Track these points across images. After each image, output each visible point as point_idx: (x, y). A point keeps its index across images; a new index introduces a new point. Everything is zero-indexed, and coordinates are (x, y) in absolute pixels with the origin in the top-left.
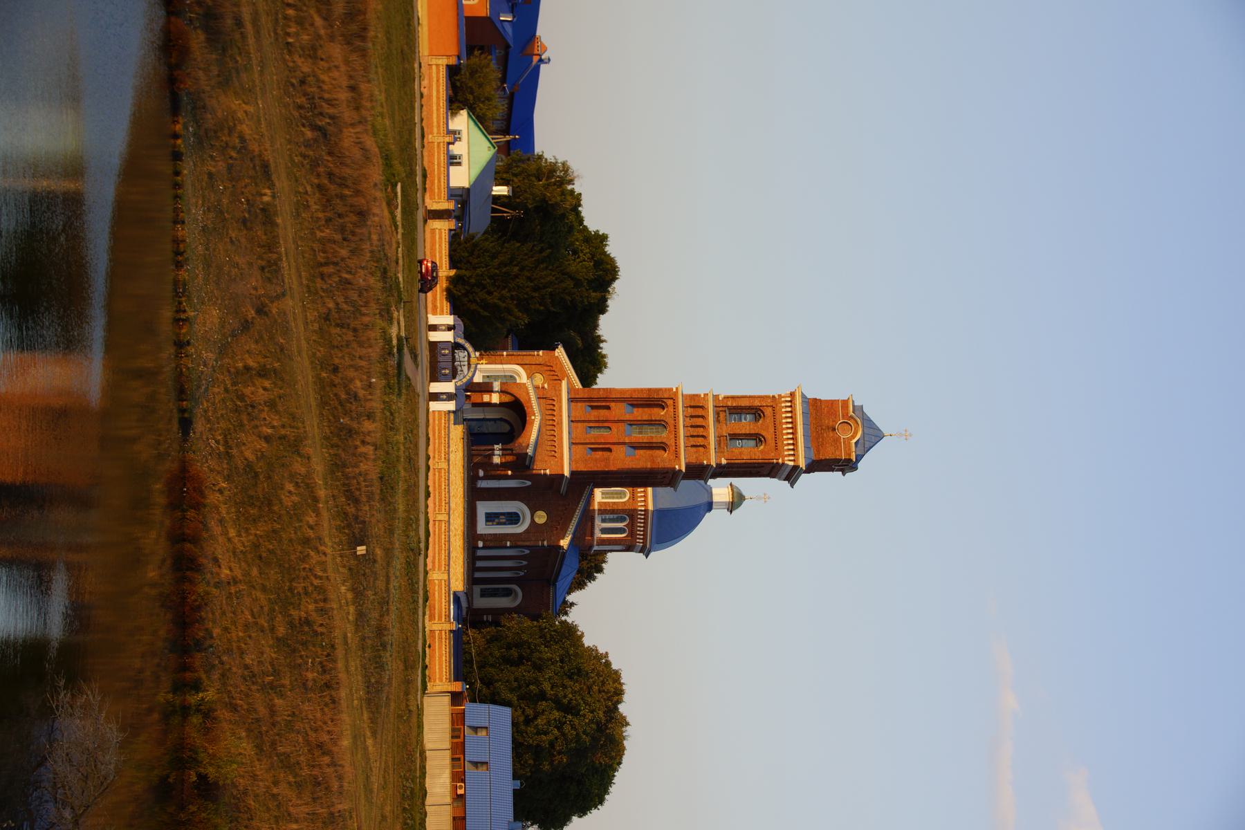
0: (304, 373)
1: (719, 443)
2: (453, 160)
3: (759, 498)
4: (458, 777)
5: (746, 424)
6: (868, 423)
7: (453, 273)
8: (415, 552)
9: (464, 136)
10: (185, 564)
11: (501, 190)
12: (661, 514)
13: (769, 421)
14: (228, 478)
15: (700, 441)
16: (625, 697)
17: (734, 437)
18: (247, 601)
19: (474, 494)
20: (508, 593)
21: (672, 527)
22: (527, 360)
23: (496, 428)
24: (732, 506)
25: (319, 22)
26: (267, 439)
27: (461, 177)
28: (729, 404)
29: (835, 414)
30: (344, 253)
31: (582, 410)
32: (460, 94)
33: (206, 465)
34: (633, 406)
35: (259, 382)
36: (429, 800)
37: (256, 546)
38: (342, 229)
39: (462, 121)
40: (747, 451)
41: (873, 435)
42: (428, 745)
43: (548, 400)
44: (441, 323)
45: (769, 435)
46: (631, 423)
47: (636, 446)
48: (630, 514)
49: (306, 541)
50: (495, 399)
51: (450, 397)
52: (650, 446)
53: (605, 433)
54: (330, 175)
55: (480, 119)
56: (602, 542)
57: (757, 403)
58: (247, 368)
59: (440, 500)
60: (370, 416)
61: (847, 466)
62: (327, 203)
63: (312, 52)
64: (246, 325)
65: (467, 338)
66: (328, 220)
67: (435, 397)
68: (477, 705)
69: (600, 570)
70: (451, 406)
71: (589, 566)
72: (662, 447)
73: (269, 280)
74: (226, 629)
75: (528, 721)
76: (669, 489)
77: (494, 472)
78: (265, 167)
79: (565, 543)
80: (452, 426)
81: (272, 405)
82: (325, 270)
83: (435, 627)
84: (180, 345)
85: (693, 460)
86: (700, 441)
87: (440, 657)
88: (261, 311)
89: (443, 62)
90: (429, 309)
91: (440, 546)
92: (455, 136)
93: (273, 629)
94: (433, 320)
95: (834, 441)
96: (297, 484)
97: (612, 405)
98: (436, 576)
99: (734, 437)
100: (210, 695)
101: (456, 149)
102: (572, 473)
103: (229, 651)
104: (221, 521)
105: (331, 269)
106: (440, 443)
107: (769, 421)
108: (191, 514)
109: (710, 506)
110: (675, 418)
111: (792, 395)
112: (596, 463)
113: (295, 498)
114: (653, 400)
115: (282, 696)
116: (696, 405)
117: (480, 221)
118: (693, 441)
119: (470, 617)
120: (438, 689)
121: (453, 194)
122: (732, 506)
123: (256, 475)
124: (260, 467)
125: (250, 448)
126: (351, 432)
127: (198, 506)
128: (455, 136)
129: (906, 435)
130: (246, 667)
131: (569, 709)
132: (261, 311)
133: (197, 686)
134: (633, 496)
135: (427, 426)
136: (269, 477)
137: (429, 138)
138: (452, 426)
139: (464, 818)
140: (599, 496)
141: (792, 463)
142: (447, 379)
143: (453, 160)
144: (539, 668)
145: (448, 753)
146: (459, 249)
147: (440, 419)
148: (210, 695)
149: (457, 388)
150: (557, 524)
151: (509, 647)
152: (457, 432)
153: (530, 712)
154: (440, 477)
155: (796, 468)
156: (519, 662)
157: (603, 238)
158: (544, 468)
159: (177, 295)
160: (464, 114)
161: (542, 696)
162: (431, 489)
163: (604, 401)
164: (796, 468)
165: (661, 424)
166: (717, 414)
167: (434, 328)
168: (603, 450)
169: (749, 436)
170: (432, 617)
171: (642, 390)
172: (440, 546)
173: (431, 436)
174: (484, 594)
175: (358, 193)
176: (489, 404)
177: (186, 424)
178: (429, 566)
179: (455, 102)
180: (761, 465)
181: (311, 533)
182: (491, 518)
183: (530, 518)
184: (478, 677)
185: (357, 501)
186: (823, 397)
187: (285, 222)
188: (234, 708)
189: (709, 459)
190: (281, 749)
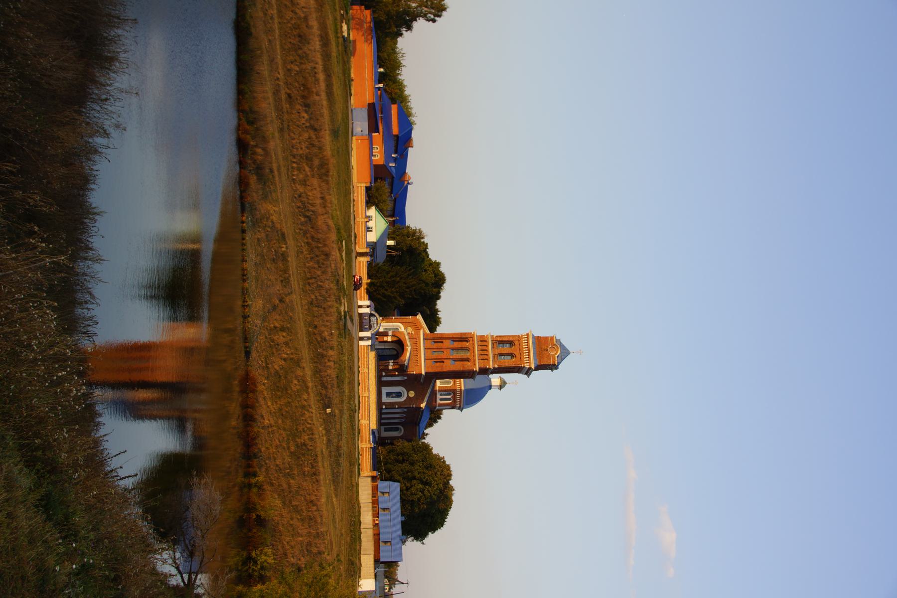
0: (301, 329)
2: (369, 229)
4: (376, 515)
5: (506, 349)
6: (563, 347)
7: (369, 281)
8: (353, 411)
9: (374, 218)
10: (248, 418)
11: (391, 243)
12: (468, 391)
14: (267, 378)
15: (485, 357)
16: (453, 477)
17: (501, 355)
18: (277, 435)
19: (380, 384)
20: (397, 429)
21: (473, 397)
22: (404, 321)
23: (390, 352)
24: (501, 387)
25: (307, 169)
26: (285, 360)
27: (372, 237)
29: (547, 343)
30: (319, 273)
31: (430, 343)
32: (371, 199)
33: (257, 373)
35: (280, 333)
36: (362, 526)
37: (280, 410)
38: (318, 262)
39: (372, 212)
40: (507, 361)
41: (565, 353)
42: (361, 501)
43: (414, 339)
44: (364, 304)
45: (517, 354)
46: (453, 349)
47: (455, 360)
48: (453, 392)
49: (303, 407)
50: (390, 339)
51: (368, 338)
52: (462, 360)
53: (441, 354)
54: (313, 238)
55: (381, 211)
56: (440, 405)
57: (511, 339)
58: (275, 327)
60: (332, 348)
61: (553, 367)
62: (311, 250)
63: (304, 183)
64: (275, 307)
65: (376, 311)
66: (312, 258)
67: (362, 339)
69: (440, 418)
70: (369, 343)
71: (435, 416)
72: (468, 360)
73: (285, 286)
74: (267, 448)
75: (407, 489)
77: (389, 373)
78: (283, 234)
79: (423, 406)
81: (287, 344)
82: (311, 281)
84: (245, 317)
85: (482, 366)
86: (485, 357)
88: (281, 301)
89: (364, 185)
92: (369, 218)
93: (289, 448)
94: (360, 303)
95: (547, 356)
96: (299, 381)
98: (363, 422)
99: (501, 355)
100: (261, 478)
101: (370, 224)
103: (269, 458)
104: (264, 398)
105: (313, 281)
107: (517, 347)
108: (251, 395)
109: (490, 387)
111: (527, 335)
112: (437, 368)
113: (298, 387)
114: (463, 338)
115: (293, 479)
116: (483, 340)
117: (381, 257)
118: (482, 357)
119: (379, 441)
121: (369, 245)
122: (501, 387)
123: (280, 377)
124: (282, 373)
125: (277, 364)
126: (323, 356)
127: (254, 391)
128: (369, 218)
129: (580, 352)
130: (277, 465)
131: (427, 483)
132: (281, 301)
133: (255, 475)
134: (455, 383)
136: (286, 377)
137: (357, 219)
140: (439, 383)
143: (369, 229)
144: (412, 464)
145: (371, 505)
146: (372, 270)
148: (261, 478)
150: (419, 397)
151: (398, 455)
152: (372, 355)
153: (408, 485)
155: (530, 369)
156: (403, 461)
157: (439, 264)
158: (413, 371)
159: (243, 294)
160: (373, 208)
161: (414, 478)
163: (440, 339)
164: (530, 369)
165: (466, 349)
166: (493, 344)
167: (361, 307)
169: (508, 354)
170: (362, 442)
174: (386, 430)
175: (325, 245)
176: (387, 342)
177: (248, 354)
179: (369, 203)
180: (514, 368)
181: (306, 403)
182: (388, 394)
183: (407, 394)
184: (384, 469)
185: (326, 388)
187: (292, 260)
188: (272, 485)
190: (294, 503)
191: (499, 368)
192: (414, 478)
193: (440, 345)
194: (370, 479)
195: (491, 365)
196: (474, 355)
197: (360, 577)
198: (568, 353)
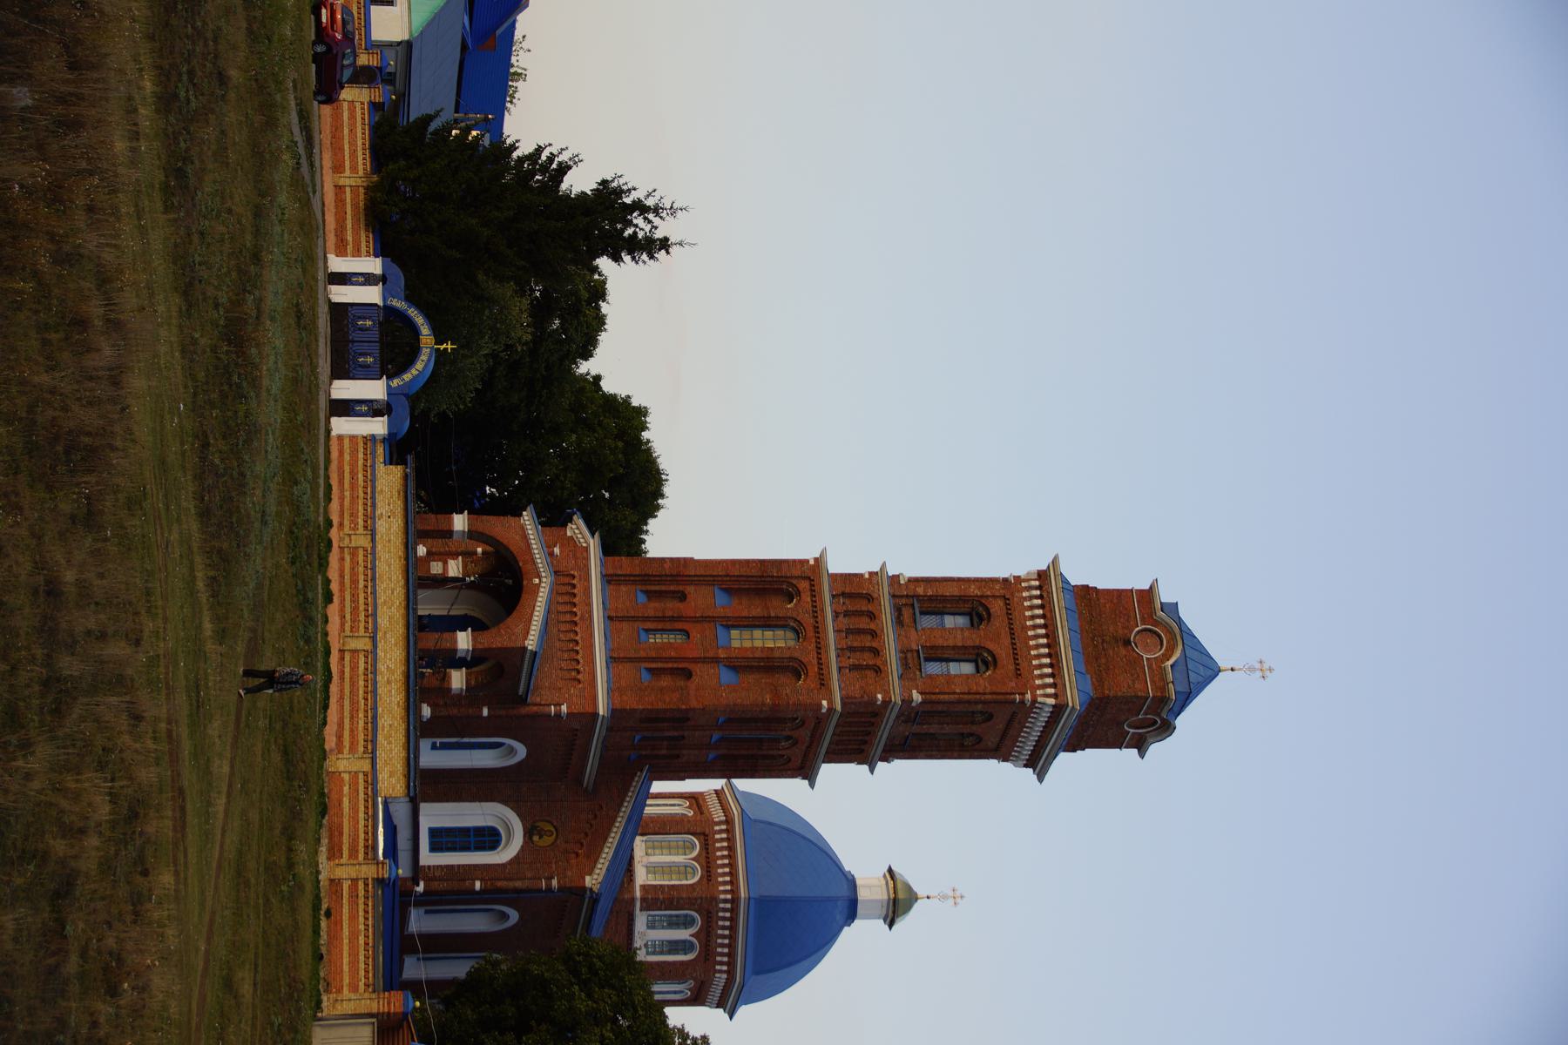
1: (904, 663)
3: (944, 897)
13: (999, 622)
17: (936, 654)
19: (417, 730)
24: (897, 905)
28: (920, 591)
34: (728, 591)
41: (1200, 671)
44: (358, 277)
45: (1002, 650)
50: (454, 568)
51: (373, 409)
57: (974, 590)
59: (355, 610)
65: (408, 299)
67: (345, 408)
70: (378, 427)
72: (794, 668)
76: (799, 784)
80: (381, 468)
83: (341, 873)
87: (354, 936)
90: (331, 239)
91: (354, 703)
94: (337, 264)
97: (690, 589)
98: (345, 764)
102: (615, 713)
106: (354, 499)
107: (999, 622)
109: (851, 912)
110: (816, 611)
111: (1042, 576)
112: (665, 696)
114: (770, 586)
116: (857, 593)
120: (348, 1008)
129: (1263, 670)
135: (326, 469)
138: (381, 468)
141: (1052, 701)
142: (367, 374)
147: (354, 453)
149: (391, 392)
152: (390, 479)
154: (354, 564)
162: (334, 587)
166: (898, 610)
167: (343, 279)
168: (672, 672)
171: (747, 562)
172: (354, 703)
173: (334, 482)
176: (442, 581)
178: (330, 742)
182: (444, 839)
186: (1102, 583)
189: (886, 692)
191: (931, 711)
193: (671, 607)
195: (896, 689)
196: (820, 648)
198: (1212, 671)
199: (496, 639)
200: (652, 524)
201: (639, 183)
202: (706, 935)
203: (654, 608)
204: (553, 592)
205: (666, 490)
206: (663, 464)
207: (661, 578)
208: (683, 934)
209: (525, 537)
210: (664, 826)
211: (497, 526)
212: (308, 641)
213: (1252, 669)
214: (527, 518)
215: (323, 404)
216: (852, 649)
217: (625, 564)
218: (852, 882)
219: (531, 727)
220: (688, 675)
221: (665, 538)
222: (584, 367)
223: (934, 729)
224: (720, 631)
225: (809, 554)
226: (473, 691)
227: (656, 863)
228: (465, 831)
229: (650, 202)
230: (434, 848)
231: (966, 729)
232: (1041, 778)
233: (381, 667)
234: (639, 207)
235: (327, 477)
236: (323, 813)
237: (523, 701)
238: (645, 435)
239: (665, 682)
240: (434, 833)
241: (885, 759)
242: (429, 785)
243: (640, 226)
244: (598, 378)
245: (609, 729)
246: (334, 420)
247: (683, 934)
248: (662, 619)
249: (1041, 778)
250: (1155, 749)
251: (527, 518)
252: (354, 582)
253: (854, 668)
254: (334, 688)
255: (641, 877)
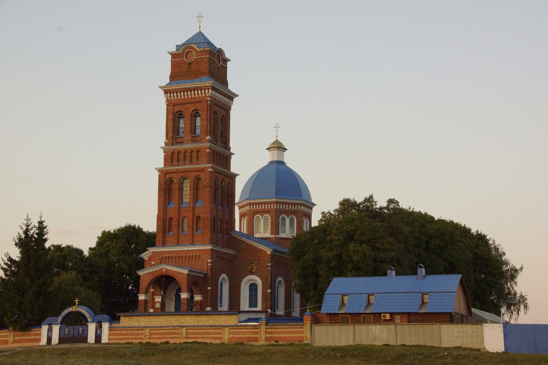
4: (377, 318)
13: (182, 108)
19: (215, 311)
24: (279, 147)
28: (171, 135)
34: (169, 202)
36: (392, 343)
42: (351, 342)
44: (49, 333)
45: (192, 107)
50: (158, 299)
57: (171, 116)
59: (172, 333)
65: (58, 315)
67: (98, 338)
68: (323, 305)
70: (106, 326)
72: (198, 179)
76: (237, 179)
83: (263, 338)
87: (284, 333)
91: (205, 333)
94: (44, 341)
97: (168, 216)
98: (226, 336)
102: (211, 243)
106: (132, 334)
107: (182, 108)
109: (281, 163)
110: (177, 172)
111: (166, 92)
112: (206, 226)
114: (168, 188)
116: (171, 157)
118: (195, 160)
120: (308, 334)
135: (120, 344)
139: (409, 314)
141: (210, 91)
142: (86, 331)
145: (357, 327)
147: (115, 334)
149: (93, 321)
152: (125, 321)
154: (156, 334)
161: (339, 257)
162: (163, 341)
163: (164, 220)
166: (177, 143)
167: (49, 340)
168: (197, 223)
170: (256, 340)
172: (205, 333)
173: (125, 341)
176: (163, 304)
178: (218, 342)
182: (253, 302)
186: (169, 72)
189: (206, 148)
191: (213, 133)
192: (339, 257)
193: (174, 223)
194: (317, 328)
195: (205, 144)
197: (479, 350)
198: (200, 34)
199: (184, 284)
200: (145, 230)
201: (17, 231)
202: (288, 213)
203: (175, 229)
204: (168, 264)
205: (132, 224)
206: (123, 225)
207: (164, 226)
208: (288, 221)
209: (148, 274)
210: (251, 227)
211: (143, 284)
212: (182, 349)
213: (200, 20)
214: (141, 273)
215: (97, 345)
216: (191, 160)
217: (159, 239)
218: (272, 162)
219: (215, 273)
220: (198, 217)
221: (149, 224)
222: (86, 253)
223: (219, 132)
224: (183, 206)
225: (156, 174)
226: (202, 292)
227: (263, 230)
228: (250, 295)
229: (25, 228)
230: (256, 306)
231: (220, 121)
232: (237, 96)
233: (193, 324)
234: (26, 232)
235: (124, 344)
236: (242, 344)
237: (206, 275)
238: (112, 232)
239: (201, 225)
240: (250, 306)
241: (229, 149)
242: (234, 307)
243: (33, 232)
244: (90, 249)
245: (217, 245)
246: (103, 342)
247: (288, 221)
248: (178, 226)
249: (237, 96)
250: (227, 55)
251: (141, 273)
252: (162, 334)
253: (197, 159)
254: (199, 340)
255: (268, 235)
